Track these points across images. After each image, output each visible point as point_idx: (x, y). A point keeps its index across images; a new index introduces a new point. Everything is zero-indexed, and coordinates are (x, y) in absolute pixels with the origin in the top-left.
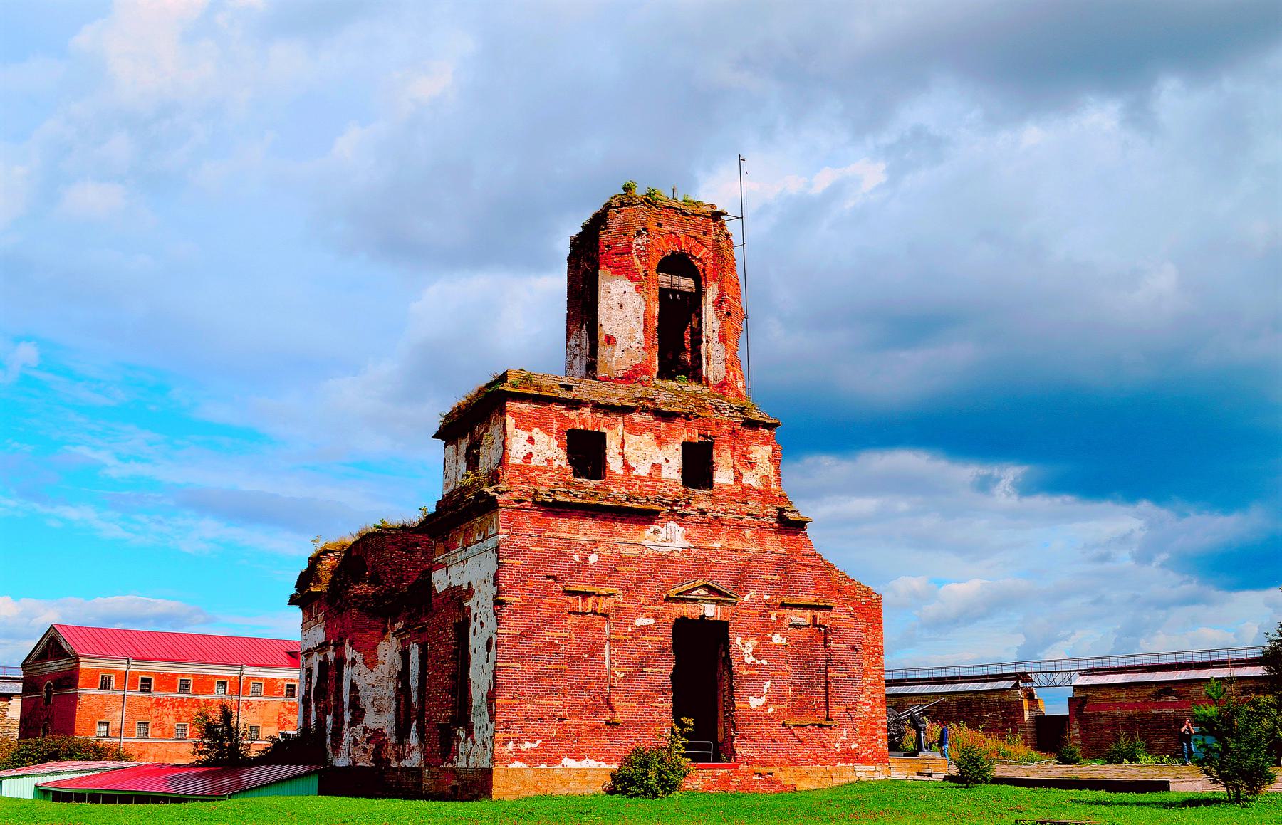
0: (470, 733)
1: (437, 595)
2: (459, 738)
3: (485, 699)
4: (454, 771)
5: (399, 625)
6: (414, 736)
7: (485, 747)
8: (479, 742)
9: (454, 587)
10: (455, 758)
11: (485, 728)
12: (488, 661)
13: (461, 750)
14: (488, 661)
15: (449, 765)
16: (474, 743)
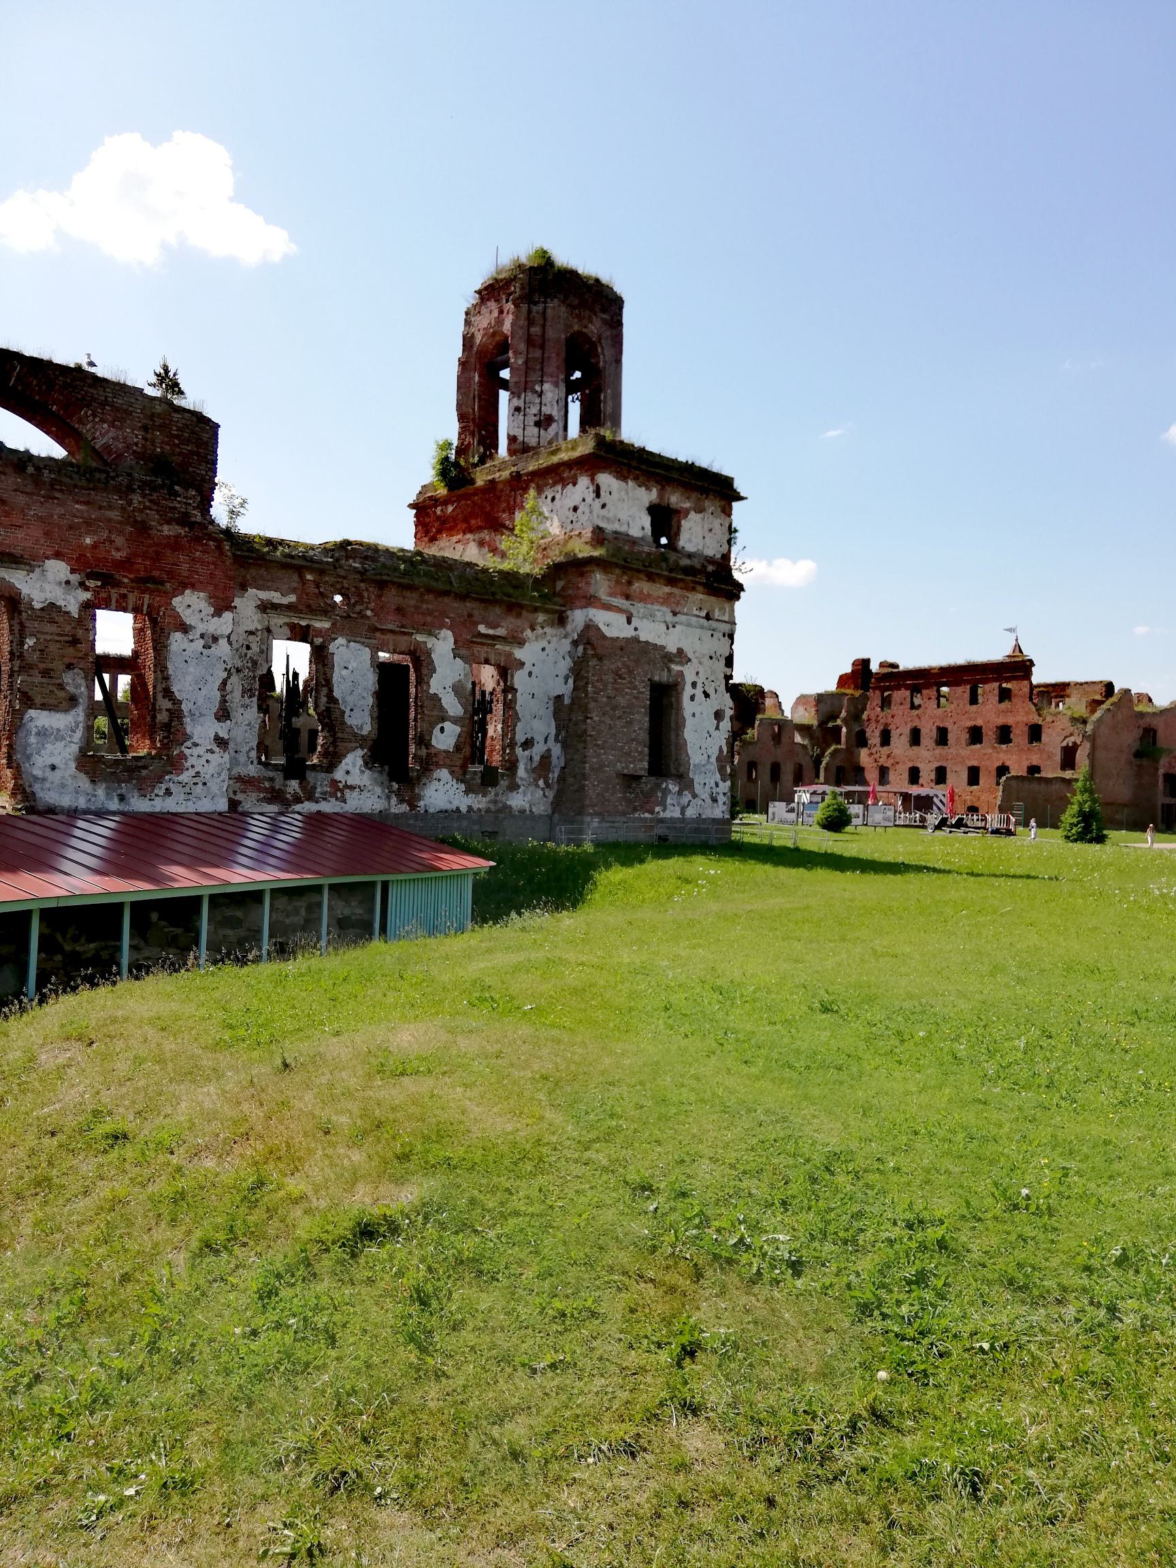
0: (686, 783)
1: (604, 637)
2: (666, 792)
3: (713, 760)
4: (662, 821)
5: (275, 597)
6: (356, 771)
7: (715, 800)
8: (706, 796)
9: (647, 642)
10: (657, 809)
11: (713, 785)
12: (717, 728)
13: (669, 801)
14: (717, 728)
15: (647, 815)
16: (695, 796)
